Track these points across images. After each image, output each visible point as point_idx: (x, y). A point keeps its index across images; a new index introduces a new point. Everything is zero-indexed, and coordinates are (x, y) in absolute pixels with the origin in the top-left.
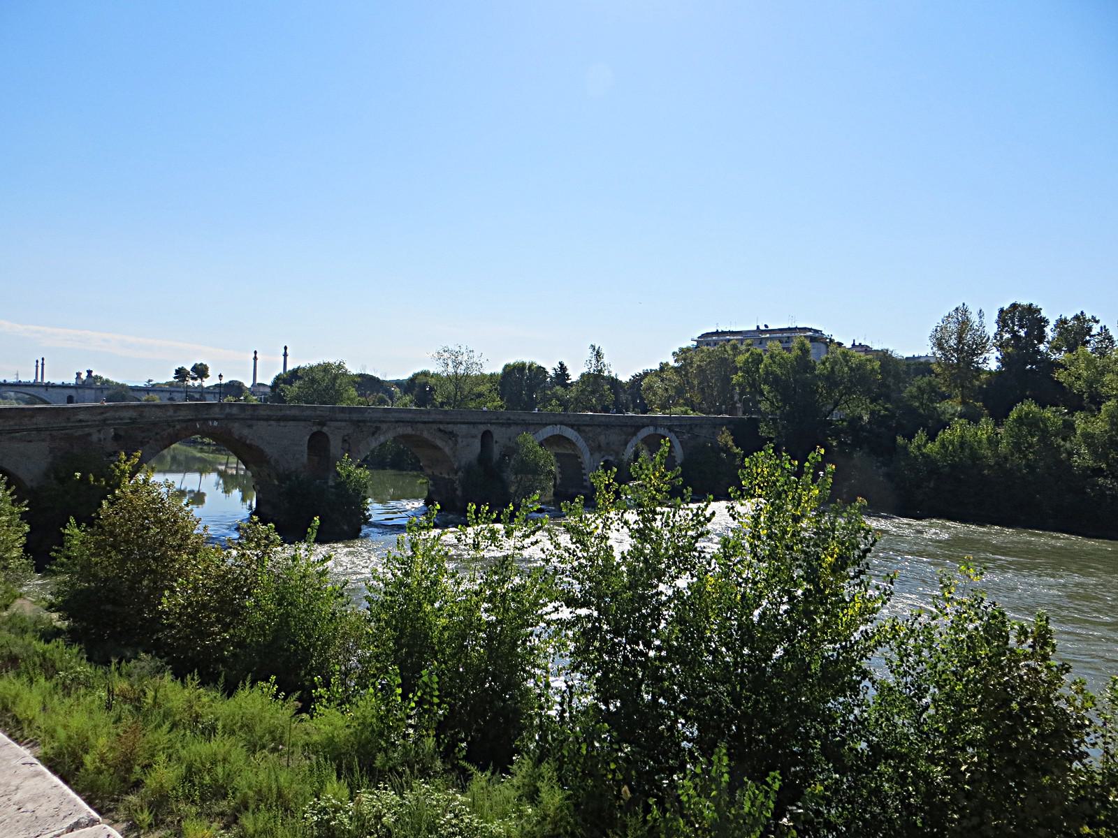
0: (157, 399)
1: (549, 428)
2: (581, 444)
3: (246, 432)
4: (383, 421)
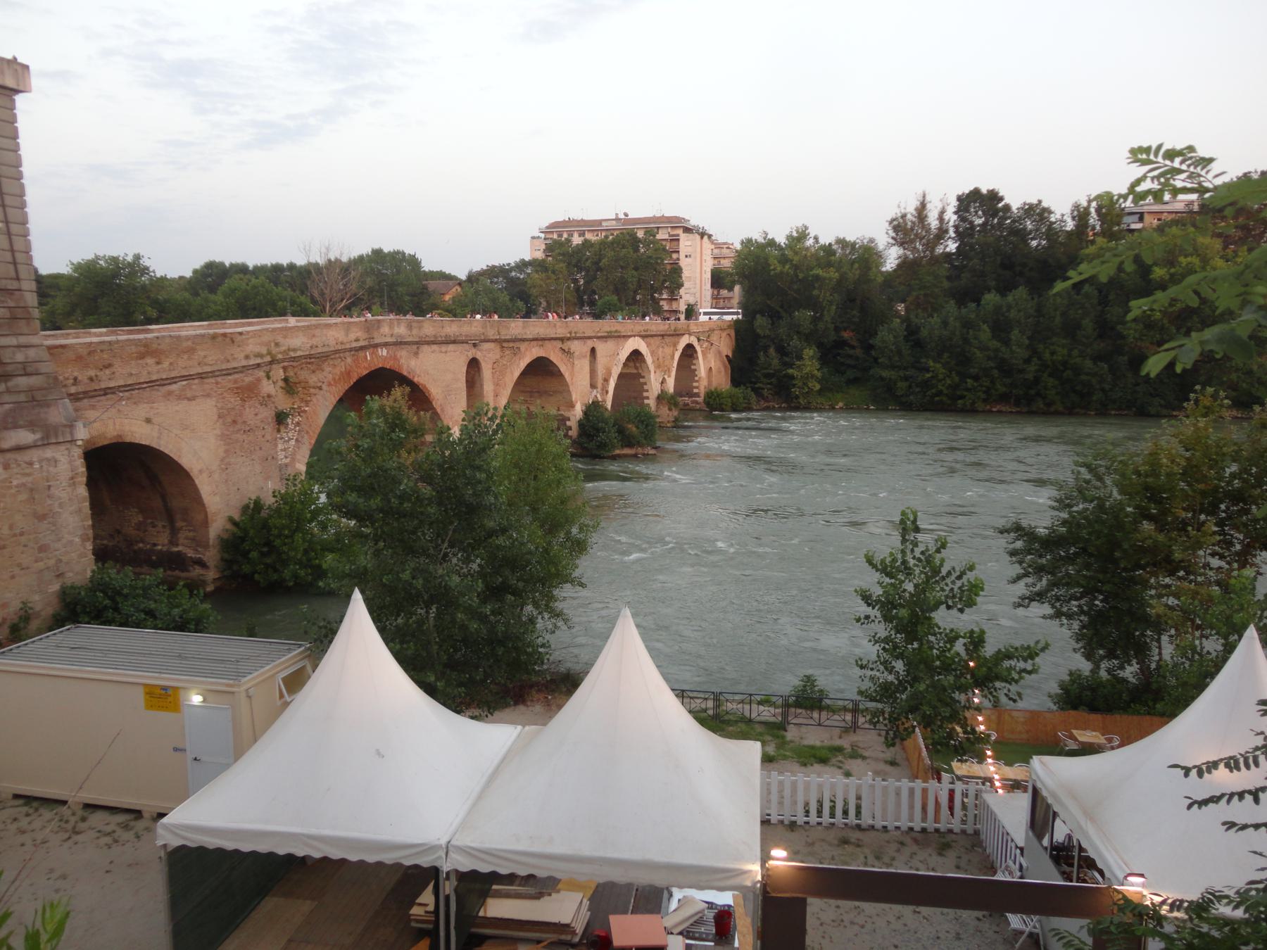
3: (413, 363)
4: (523, 340)
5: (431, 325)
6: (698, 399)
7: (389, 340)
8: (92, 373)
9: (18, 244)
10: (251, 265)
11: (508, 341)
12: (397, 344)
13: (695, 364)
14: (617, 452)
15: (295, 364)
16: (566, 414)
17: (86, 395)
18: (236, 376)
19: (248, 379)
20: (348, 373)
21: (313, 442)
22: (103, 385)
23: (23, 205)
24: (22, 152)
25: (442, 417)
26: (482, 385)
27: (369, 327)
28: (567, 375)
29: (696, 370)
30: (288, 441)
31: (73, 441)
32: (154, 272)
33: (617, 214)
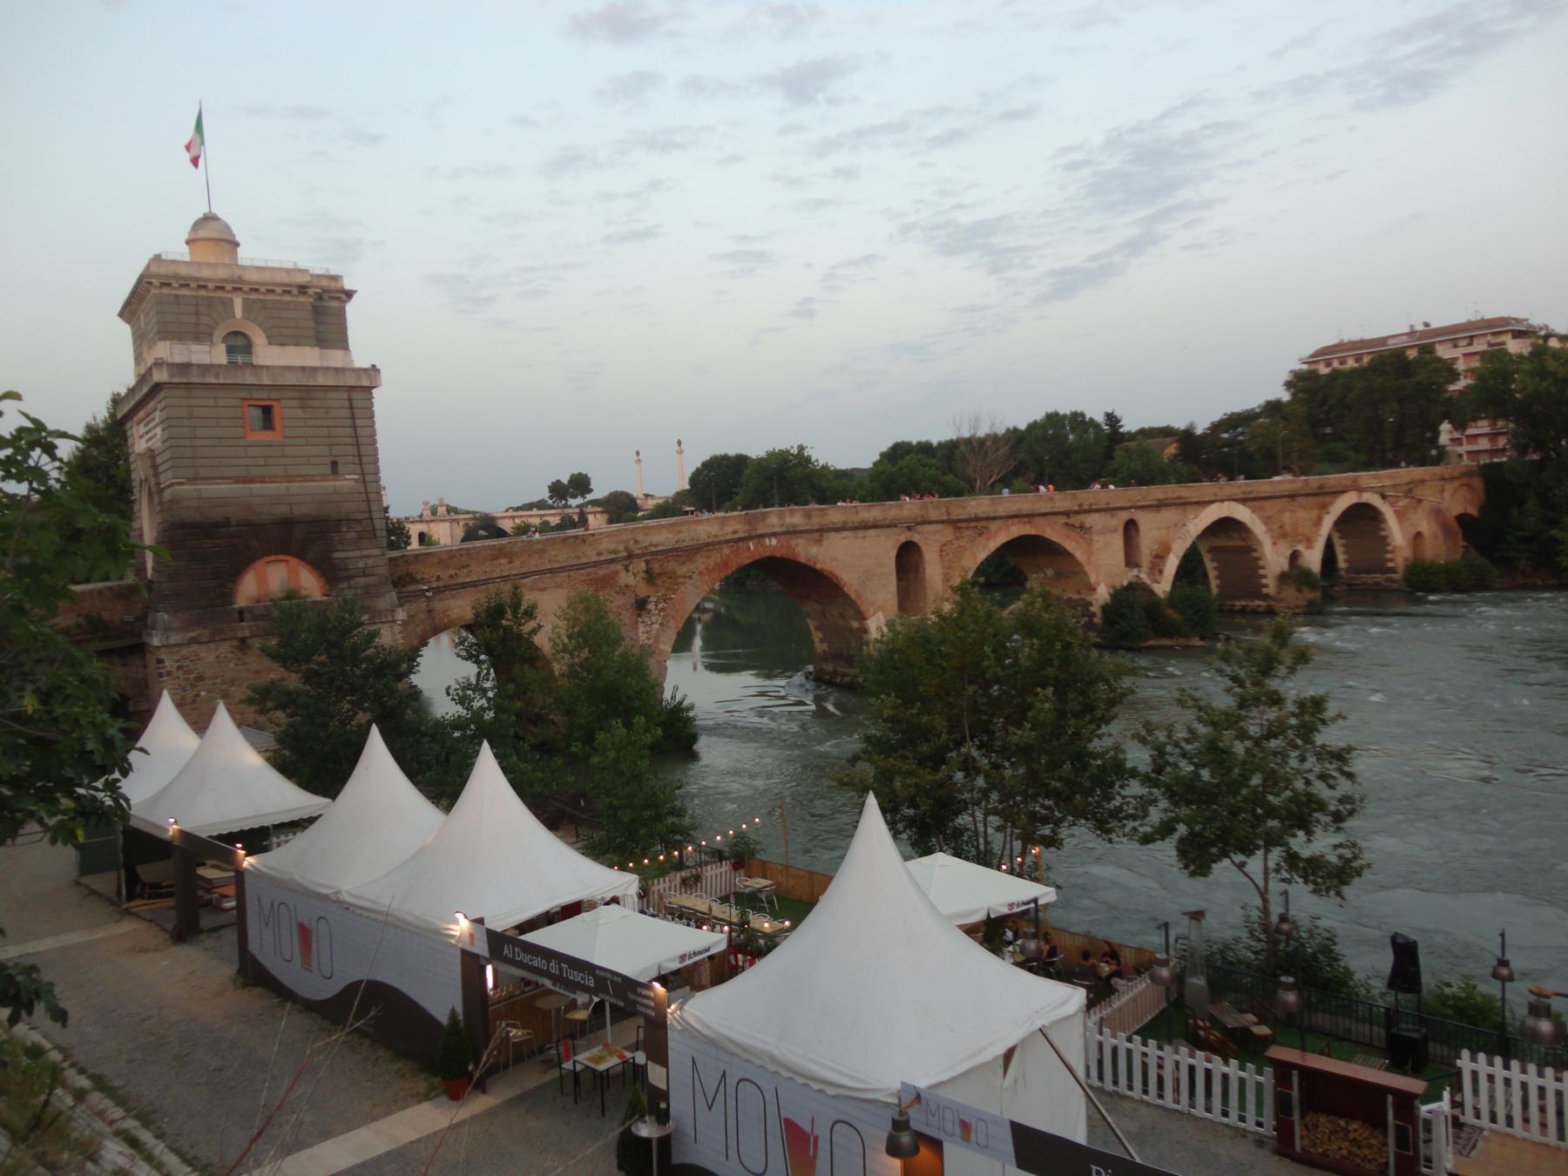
0: (1242, 434)
1: (1213, 507)
2: (1258, 527)
3: (814, 550)
4: (994, 518)
5: (838, 513)
6: (1393, 576)
7: (777, 530)
8: (452, 572)
9: (371, 487)
10: (935, 442)
11: (966, 520)
12: (787, 533)
13: (1383, 530)
14: (1152, 642)
15: (659, 557)
16: (1088, 598)
17: (447, 588)
18: (589, 570)
19: (601, 573)
20: (726, 564)
21: (680, 625)
22: (460, 581)
23: (376, 461)
24: (378, 426)
25: (859, 602)
26: (924, 569)
27: (749, 521)
28: (1079, 554)
29: (1386, 537)
30: (651, 625)
31: (394, 621)
32: (817, 461)
33: (1412, 326)
